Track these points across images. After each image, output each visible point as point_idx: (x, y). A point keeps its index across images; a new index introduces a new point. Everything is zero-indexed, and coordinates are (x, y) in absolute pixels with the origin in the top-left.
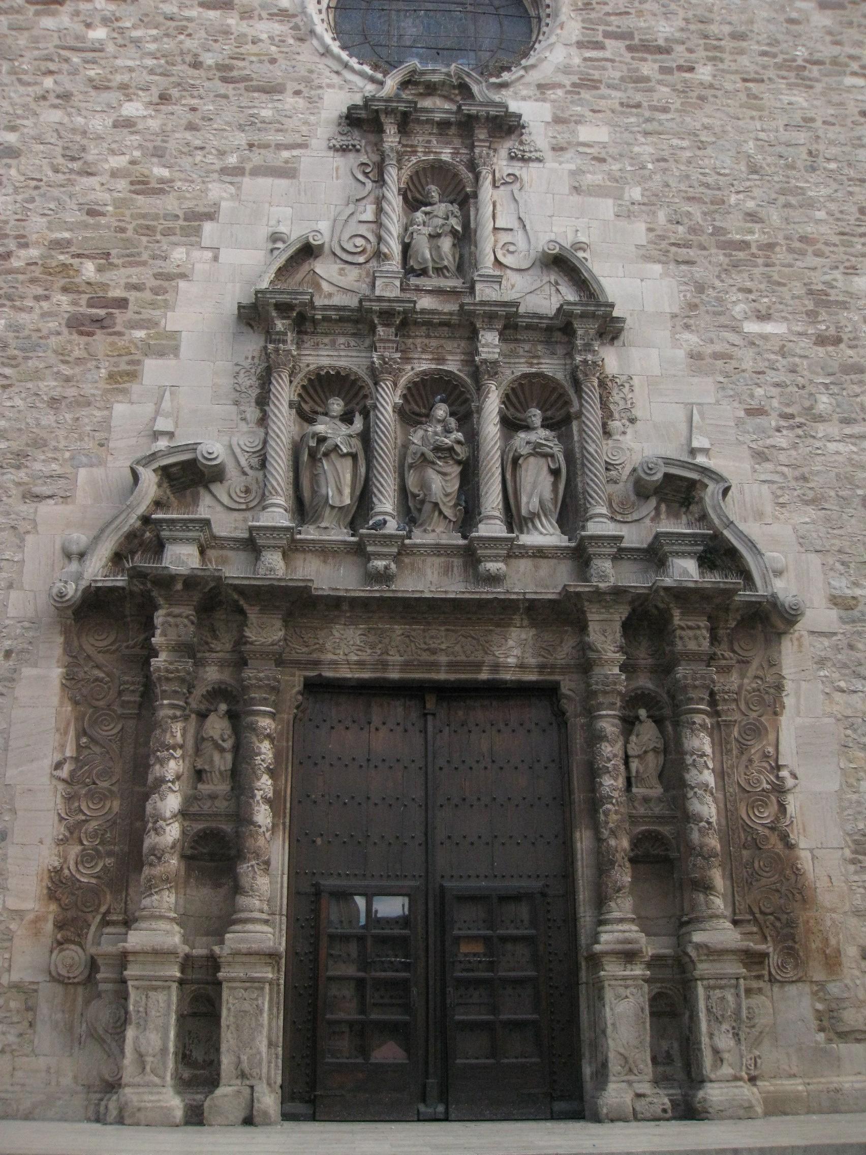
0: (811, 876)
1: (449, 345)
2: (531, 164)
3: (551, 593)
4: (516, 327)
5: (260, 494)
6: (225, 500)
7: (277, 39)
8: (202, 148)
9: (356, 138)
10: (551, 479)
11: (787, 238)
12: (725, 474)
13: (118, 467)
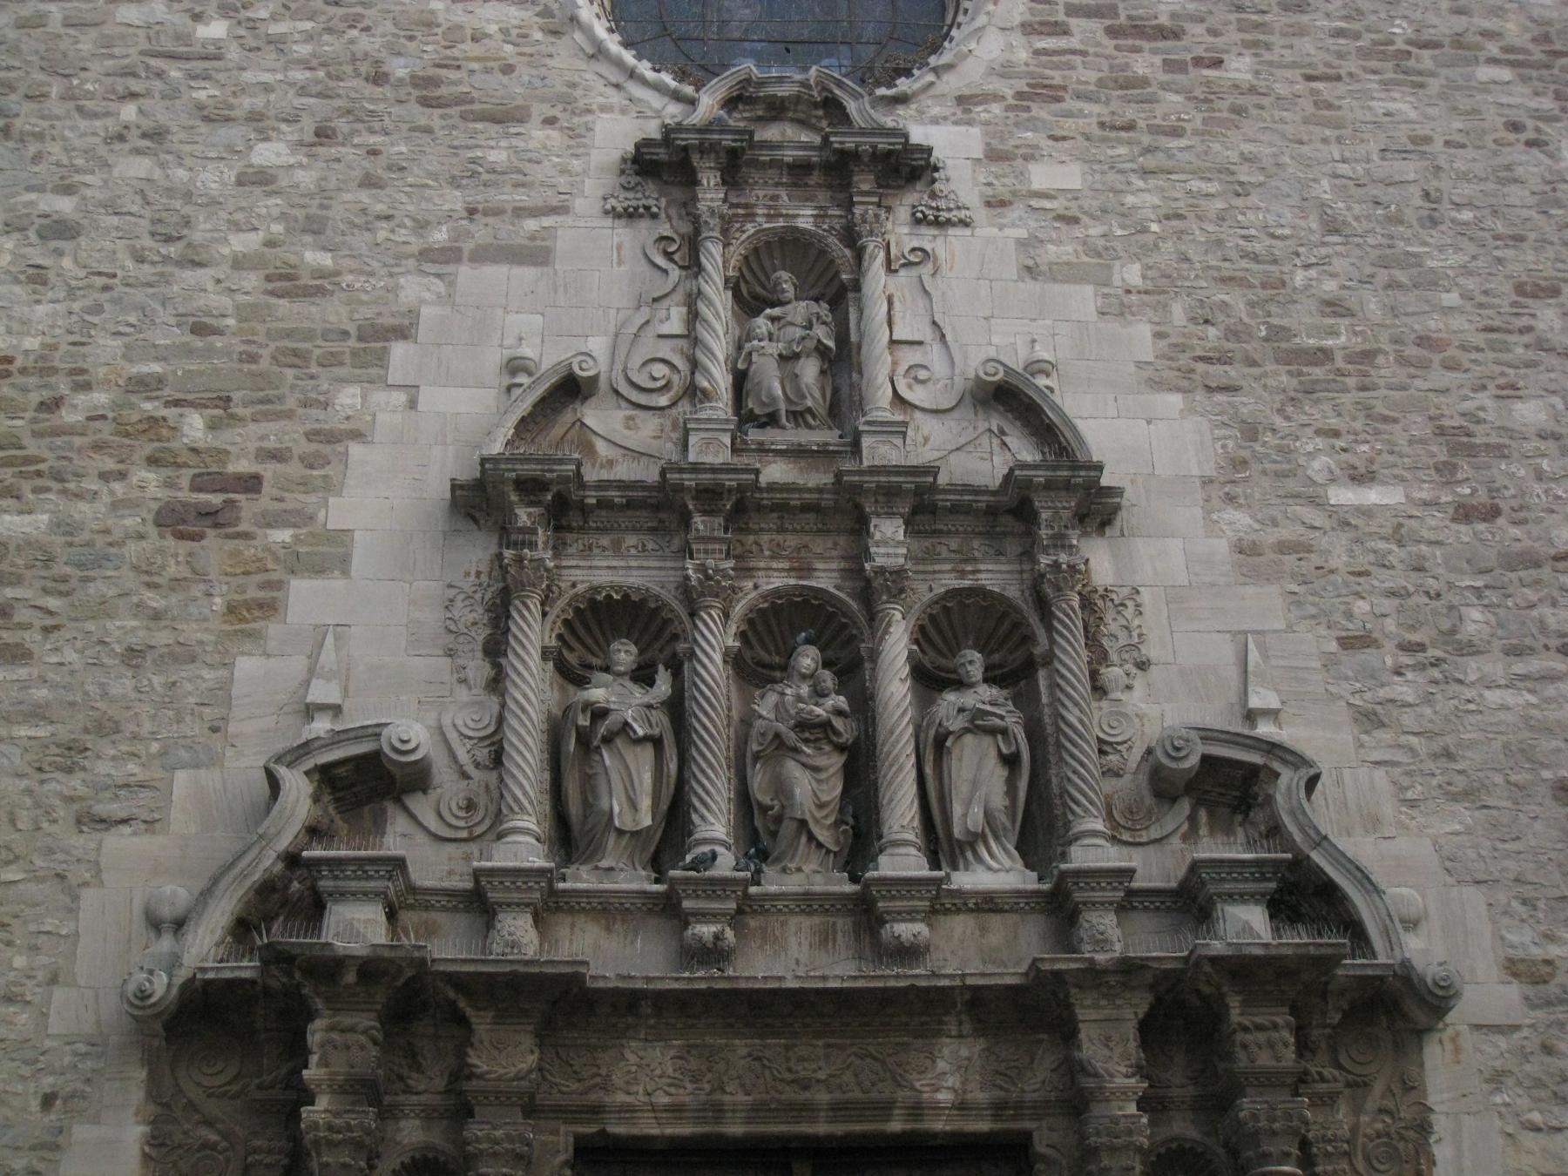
1: (819, 545)
2: (951, 231)
4: (933, 510)
5: (493, 808)
6: (432, 823)
7: (514, 32)
8: (388, 218)
9: (651, 195)
10: (1002, 773)
12: (1309, 753)
13: (244, 766)
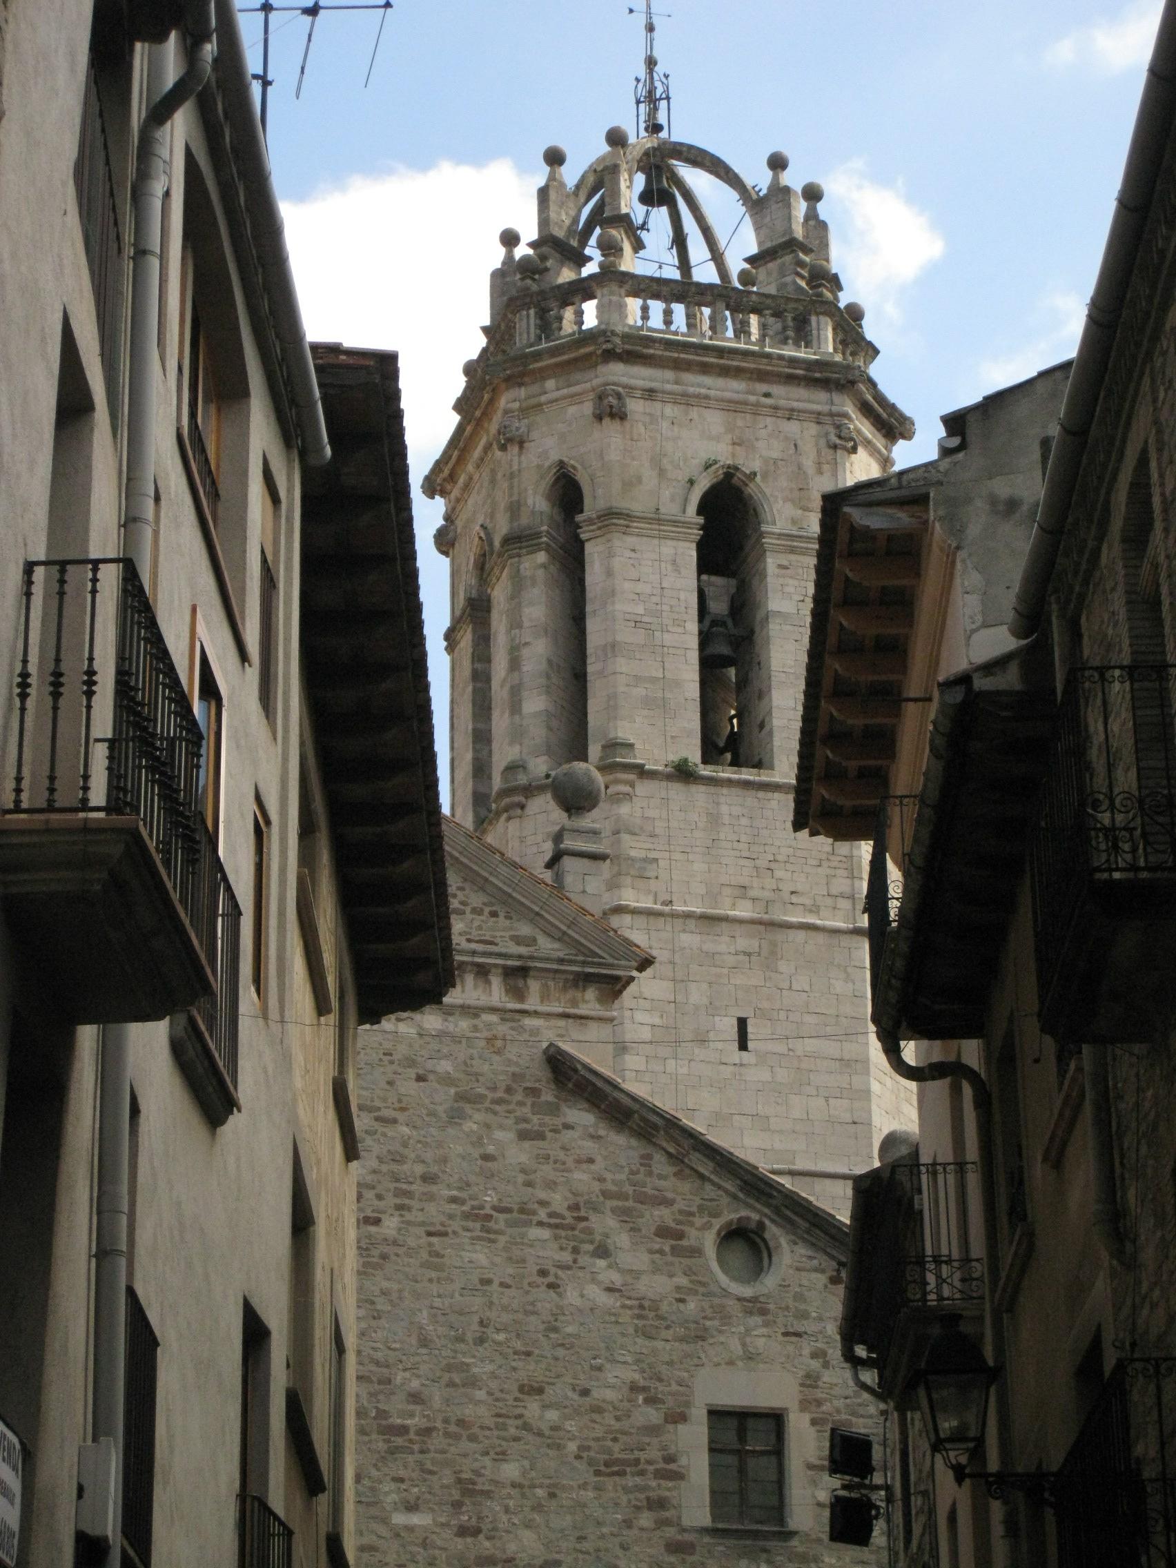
11: (446, 1421)
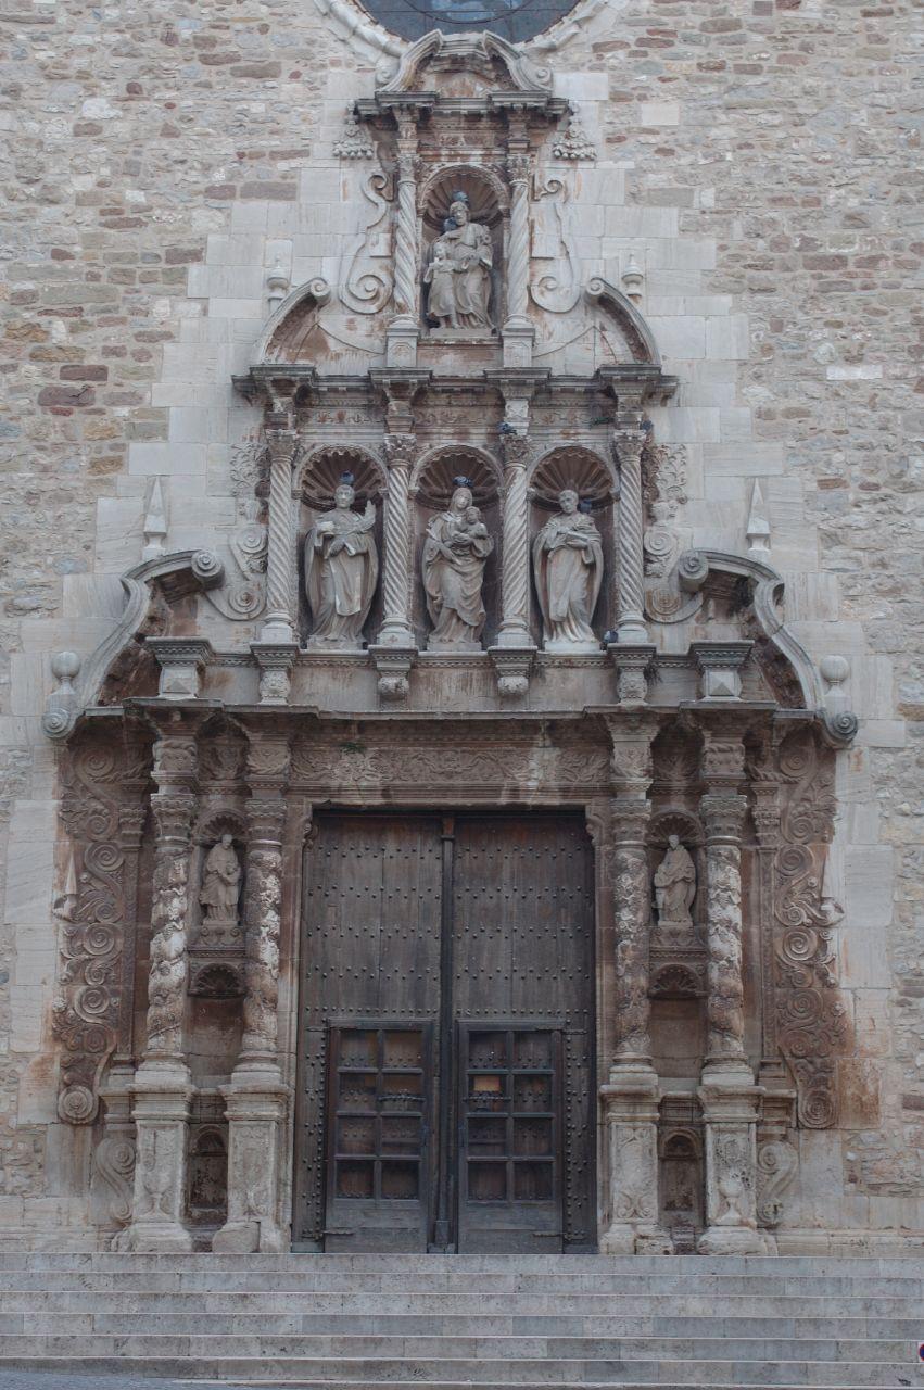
0: (851, 1017)
2: (580, 165)
3: (574, 708)
5: (262, 600)
6: (225, 609)
11: (897, 247)
12: (778, 570)
